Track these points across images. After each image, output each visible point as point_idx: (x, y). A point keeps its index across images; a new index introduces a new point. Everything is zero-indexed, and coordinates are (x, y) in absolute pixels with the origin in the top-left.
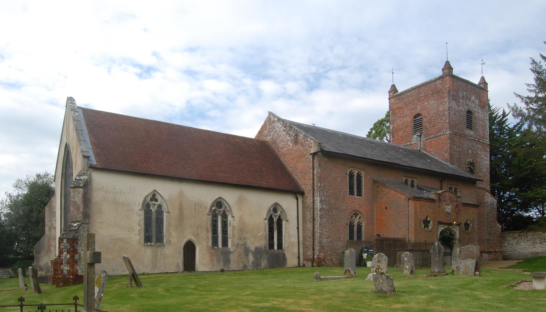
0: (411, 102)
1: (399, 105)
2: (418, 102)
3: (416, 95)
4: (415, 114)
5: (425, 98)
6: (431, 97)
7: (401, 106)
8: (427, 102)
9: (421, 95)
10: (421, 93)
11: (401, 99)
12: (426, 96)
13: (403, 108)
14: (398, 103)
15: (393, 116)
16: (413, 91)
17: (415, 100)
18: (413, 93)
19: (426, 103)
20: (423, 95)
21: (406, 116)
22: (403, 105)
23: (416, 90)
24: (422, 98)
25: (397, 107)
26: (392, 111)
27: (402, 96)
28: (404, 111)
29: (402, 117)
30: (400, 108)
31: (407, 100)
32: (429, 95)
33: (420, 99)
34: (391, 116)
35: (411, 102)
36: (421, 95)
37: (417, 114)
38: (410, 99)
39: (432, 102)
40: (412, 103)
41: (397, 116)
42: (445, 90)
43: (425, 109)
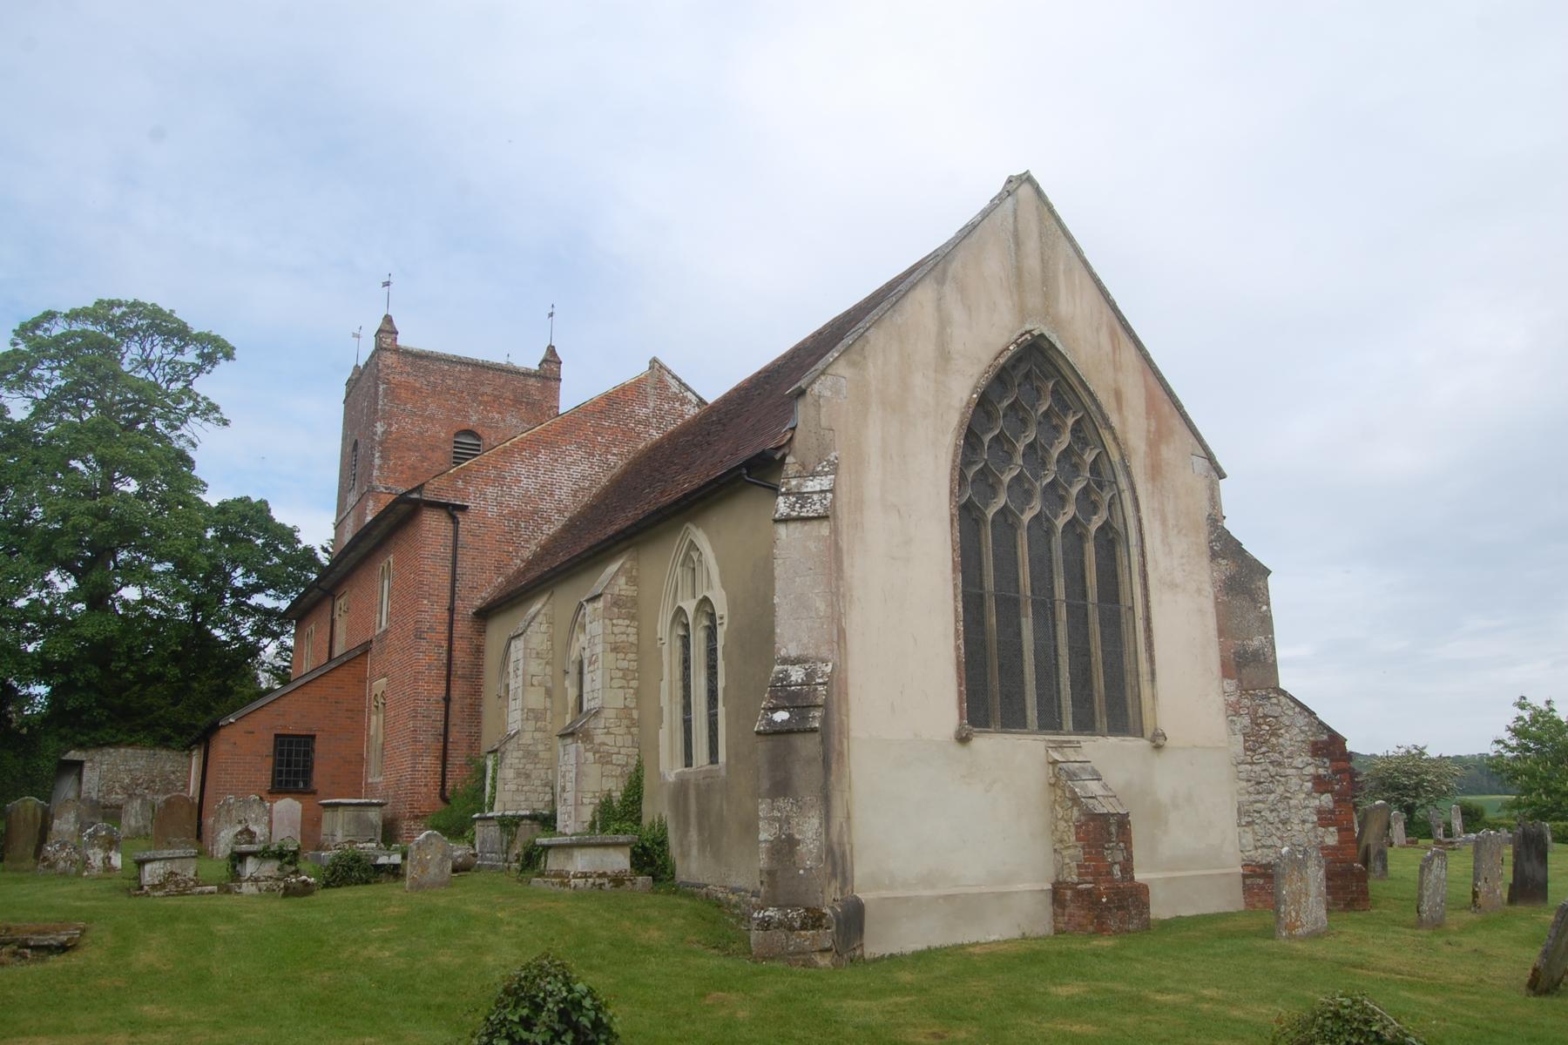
0: (451, 392)
1: (411, 379)
2: (473, 402)
3: (470, 383)
4: (463, 428)
5: (494, 401)
6: (512, 409)
7: (418, 385)
8: (499, 413)
9: (482, 389)
10: (482, 384)
11: (422, 370)
12: (497, 398)
13: (424, 394)
14: (408, 375)
15: (391, 401)
16: (459, 367)
17: (462, 392)
18: (460, 371)
19: (497, 416)
20: (488, 390)
21: (431, 418)
22: (426, 387)
23: (470, 369)
24: (486, 398)
25: (407, 384)
26: (385, 386)
27: (425, 363)
28: (427, 405)
29: (421, 416)
30: (414, 391)
31: (440, 382)
32: (504, 399)
33: (480, 398)
34: (381, 398)
35: (451, 392)
36: (482, 389)
37: (470, 431)
38: (450, 382)
39: (515, 421)
40: (454, 395)
41: (402, 407)
42: (549, 410)
43: (491, 427)
